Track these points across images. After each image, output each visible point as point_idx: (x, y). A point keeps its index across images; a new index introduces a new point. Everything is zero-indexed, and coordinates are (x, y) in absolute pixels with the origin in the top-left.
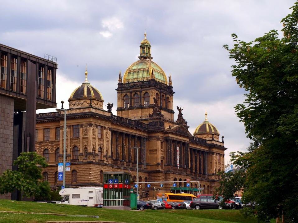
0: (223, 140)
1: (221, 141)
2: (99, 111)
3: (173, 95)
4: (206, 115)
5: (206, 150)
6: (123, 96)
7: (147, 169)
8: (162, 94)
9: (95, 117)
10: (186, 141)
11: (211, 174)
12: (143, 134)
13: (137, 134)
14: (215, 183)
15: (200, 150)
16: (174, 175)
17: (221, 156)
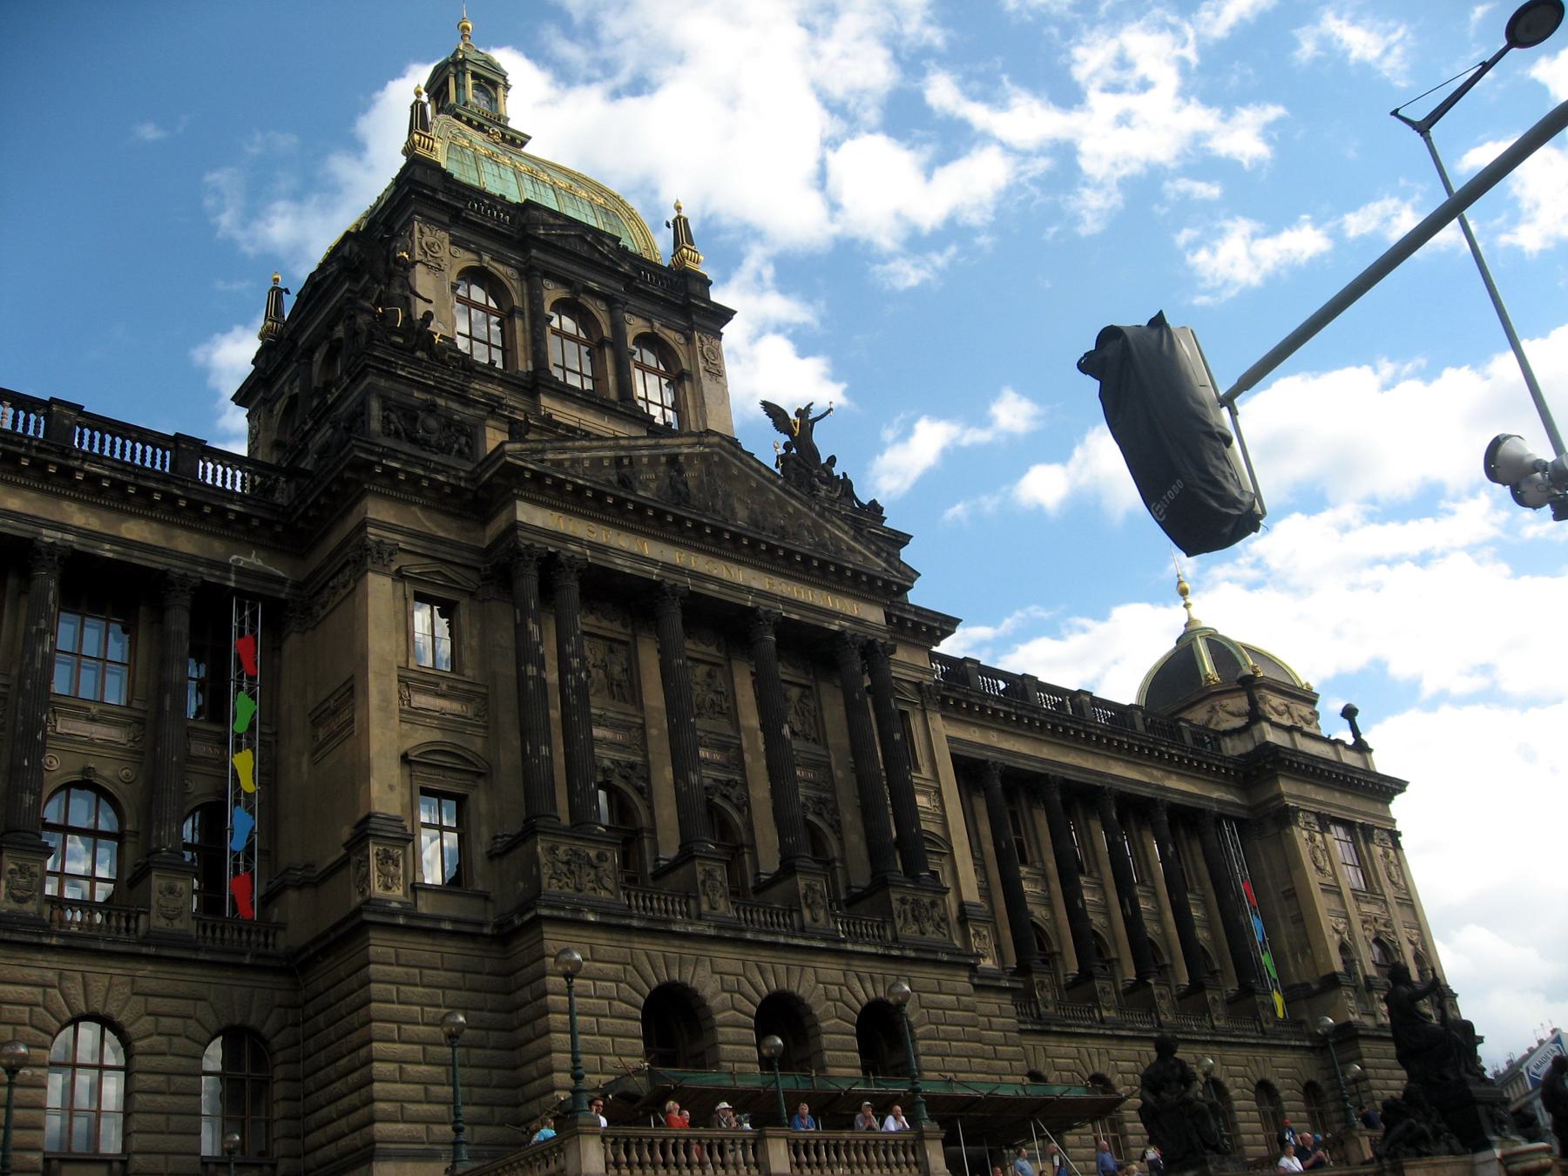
0: (1356, 732)
3: (719, 336)
4: (1184, 593)
5: (1218, 801)
6: (275, 422)
7: (281, 926)
8: (552, 293)
10: (835, 615)
11: (1315, 987)
12: (186, 542)
16: (643, 948)
17: (1368, 838)
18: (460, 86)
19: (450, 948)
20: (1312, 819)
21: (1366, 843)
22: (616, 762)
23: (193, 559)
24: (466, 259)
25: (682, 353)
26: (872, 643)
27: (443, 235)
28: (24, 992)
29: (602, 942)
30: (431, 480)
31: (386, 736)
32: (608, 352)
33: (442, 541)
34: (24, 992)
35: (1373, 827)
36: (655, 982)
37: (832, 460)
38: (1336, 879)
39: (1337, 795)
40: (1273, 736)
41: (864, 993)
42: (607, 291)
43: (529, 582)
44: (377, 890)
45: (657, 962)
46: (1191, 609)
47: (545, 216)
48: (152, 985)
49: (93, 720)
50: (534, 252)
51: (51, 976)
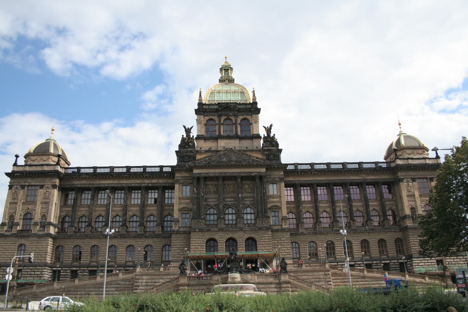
0: (437, 154)
1: (434, 156)
2: (33, 167)
4: (400, 124)
9: (14, 175)
12: (161, 181)
13: (144, 183)
14: (410, 231)
15: (359, 181)
16: (206, 233)
18: (222, 73)
19: (183, 235)
20: (409, 179)
21: (430, 182)
22: (213, 204)
23: (162, 183)
24: (207, 118)
25: (250, 120)
26: (261, 176)
27: (203, 116)
28: (140, 243)
29: (200, 233)
30: (183, 169)
31: (176, 208)
32: (234, 126)
33: (187, 177)
34: (140, 243)
35: (433, 178)
36: (208, 238)
37: (274, 135)
38: (414, 193)
39: (421, 172)
40: (399, 162)
41: (247, 236)
42: (233, 114)
43: (195, 182)
44: (174, 228)
45: (208, 235)
46: (401, 128)
47: (222, 104)
48: (156, 241)
49: (152, 207)
50: (219, 113)
51: (143, 241)
